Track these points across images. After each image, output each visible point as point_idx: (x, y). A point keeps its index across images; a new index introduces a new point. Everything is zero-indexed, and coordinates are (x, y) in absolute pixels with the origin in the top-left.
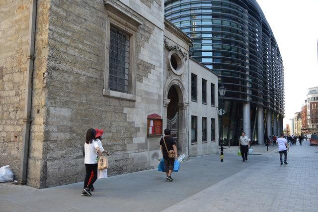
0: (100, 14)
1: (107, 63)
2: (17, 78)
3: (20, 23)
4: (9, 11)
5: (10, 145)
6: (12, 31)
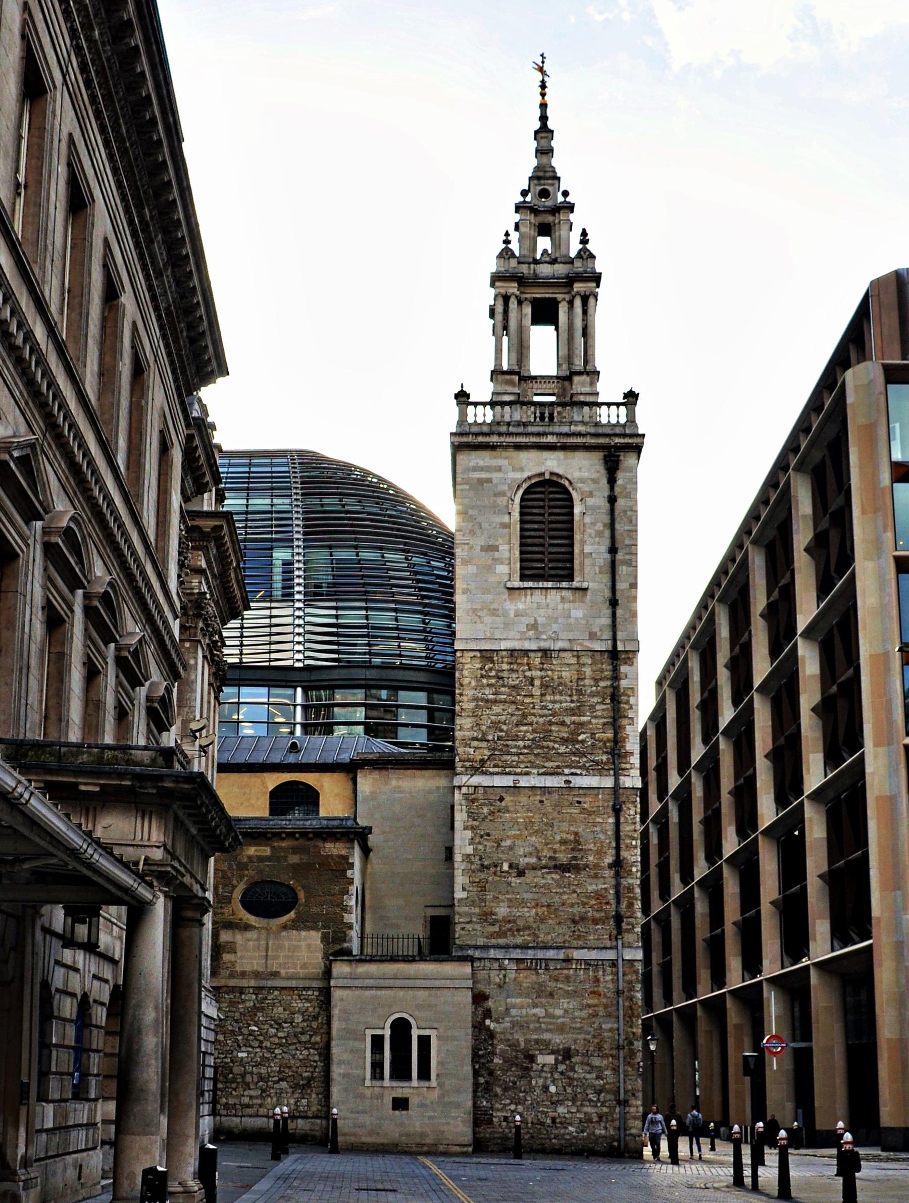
2: (596, 1062)
3: (596, 1009)
4: (575, 992)
5: (591, 1125)
6: (584, 1013)
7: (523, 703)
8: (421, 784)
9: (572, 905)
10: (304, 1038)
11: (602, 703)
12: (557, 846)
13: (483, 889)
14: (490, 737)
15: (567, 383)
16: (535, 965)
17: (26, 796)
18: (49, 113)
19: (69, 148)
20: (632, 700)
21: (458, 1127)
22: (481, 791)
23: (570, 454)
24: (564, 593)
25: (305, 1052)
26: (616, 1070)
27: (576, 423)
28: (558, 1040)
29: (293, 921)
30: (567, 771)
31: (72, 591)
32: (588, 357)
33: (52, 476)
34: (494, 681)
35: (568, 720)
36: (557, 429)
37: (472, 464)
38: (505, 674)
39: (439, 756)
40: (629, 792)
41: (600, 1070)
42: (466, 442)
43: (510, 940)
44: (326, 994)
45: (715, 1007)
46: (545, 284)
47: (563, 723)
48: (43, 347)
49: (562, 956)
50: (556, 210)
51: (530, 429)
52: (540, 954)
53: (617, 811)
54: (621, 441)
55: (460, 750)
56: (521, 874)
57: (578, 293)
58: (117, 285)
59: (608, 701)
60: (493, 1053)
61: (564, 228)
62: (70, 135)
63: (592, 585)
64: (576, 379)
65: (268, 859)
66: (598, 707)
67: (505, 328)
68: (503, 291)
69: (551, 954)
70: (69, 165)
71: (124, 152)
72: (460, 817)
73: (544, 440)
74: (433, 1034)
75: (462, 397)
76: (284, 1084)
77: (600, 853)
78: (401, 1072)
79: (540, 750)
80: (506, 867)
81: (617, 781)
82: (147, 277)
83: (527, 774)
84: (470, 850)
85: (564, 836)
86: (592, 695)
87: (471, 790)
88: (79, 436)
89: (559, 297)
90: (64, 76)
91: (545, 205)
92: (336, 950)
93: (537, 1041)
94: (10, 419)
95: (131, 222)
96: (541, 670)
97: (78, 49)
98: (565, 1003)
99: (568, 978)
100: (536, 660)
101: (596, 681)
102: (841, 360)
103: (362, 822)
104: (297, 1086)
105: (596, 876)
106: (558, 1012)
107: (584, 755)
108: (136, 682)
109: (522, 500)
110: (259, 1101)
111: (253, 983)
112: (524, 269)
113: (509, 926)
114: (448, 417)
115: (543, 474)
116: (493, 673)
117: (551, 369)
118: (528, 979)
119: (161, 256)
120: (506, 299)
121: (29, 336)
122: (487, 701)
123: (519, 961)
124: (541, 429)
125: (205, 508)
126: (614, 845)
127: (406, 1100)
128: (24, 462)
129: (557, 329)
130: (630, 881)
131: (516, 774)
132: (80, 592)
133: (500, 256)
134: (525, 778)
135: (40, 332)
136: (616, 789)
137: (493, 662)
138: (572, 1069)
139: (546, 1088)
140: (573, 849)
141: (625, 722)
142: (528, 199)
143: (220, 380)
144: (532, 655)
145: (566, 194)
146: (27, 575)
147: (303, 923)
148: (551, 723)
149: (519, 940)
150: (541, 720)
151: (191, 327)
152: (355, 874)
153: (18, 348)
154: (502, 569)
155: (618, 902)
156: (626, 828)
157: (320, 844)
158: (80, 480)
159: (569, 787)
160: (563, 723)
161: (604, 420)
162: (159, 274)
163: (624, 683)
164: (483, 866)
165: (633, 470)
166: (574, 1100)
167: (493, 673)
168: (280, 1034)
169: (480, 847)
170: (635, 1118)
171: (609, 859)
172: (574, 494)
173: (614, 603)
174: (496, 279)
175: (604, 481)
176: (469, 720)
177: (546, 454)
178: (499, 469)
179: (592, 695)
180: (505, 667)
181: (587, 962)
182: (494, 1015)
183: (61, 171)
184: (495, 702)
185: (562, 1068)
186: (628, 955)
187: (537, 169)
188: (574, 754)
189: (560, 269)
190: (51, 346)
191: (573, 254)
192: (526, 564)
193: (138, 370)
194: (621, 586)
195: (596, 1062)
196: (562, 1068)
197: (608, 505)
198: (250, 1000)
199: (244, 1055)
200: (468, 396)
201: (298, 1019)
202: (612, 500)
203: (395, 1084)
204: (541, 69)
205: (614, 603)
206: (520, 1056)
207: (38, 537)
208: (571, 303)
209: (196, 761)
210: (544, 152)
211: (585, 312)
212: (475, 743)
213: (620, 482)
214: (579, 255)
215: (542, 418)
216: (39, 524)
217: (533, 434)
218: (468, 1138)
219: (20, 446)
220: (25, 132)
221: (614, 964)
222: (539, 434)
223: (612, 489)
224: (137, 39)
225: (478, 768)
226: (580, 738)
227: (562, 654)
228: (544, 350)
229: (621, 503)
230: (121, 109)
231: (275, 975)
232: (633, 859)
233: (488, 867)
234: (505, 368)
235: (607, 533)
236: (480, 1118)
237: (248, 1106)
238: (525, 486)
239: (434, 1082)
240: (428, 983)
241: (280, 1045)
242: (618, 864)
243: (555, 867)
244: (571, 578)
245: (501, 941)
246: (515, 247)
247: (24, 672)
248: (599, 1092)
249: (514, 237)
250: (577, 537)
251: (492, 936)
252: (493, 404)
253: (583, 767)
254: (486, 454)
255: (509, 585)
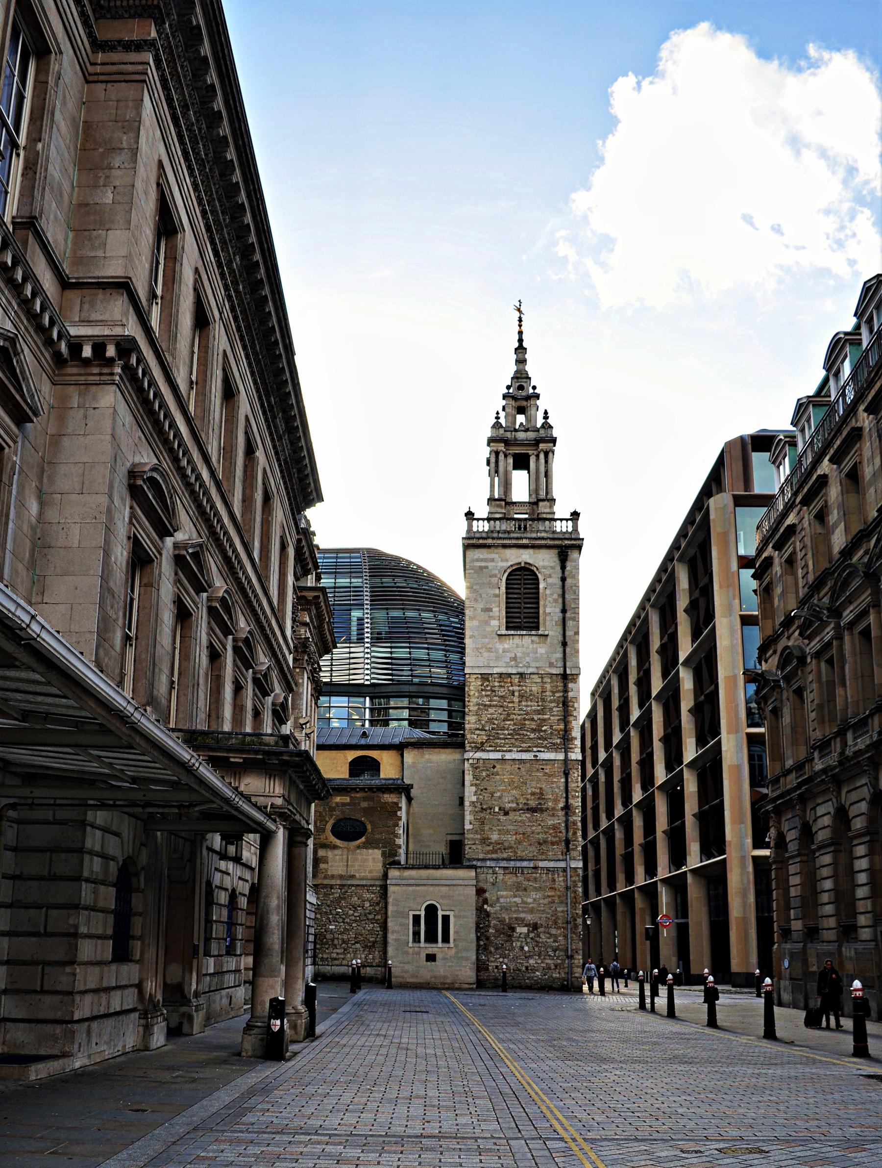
2: (553, 931)
6: (546, 901)
7: (507, 707)
8: (444, 758)
9: (538, 834)
10: (370, 917)
11: (557, 707)
12: (529, 796)
13: (483, 823)
14: (487, 728)
15: (535, 507)
16: (515, 871)
17: (197, 765)
18: (211, 337)
19: (224, 359)
20: (576, 705)
21: (468, 973)
22: (481, 762)
23: (537, 551)
24: (533, 638)
25: (371, 926)
26: (566, 937)
27: (541, 532)
28: (529, 917)
29: (364, 843)
30: (535, 749)
31: (226, 637)
32: (548, 490)
33: (213, 564)
34: (489, 693)
35: (536, 717)
36: (529, 535)
37: (476, 557)
38: (496, 689)
39: (455, 740)
40: (574, 763)
41: (556, 936)
42: (472, 543)
43: (500, 855)
44: (384, 888)
45: (628, 897)
46: (521, 444)
47: (533, 719)
48: (207, 484)
49: (532, 866)
50: (528, 398)
51: (512, 535)
52: (518, 864)
53: (566, 775)
54: (569, 542)
55: (468, 736)
56: (506, 814)
57: (542, 450)
58: (254, 445)
59: (561, 705)
60: (489, 926)
61: (534, 409)
62: (225, 351)
63: (551, 633)
64: (541, 504)
65: (348, 804)
66: (554, 709)
67: (497, 472)
68: (495, 449)
69: (525, 864)
70: (224, 370)
71: (258, 362)
72: (468, 778)
73: (520, 542)
74: (451, 914)
75: (469, 515)
76: (358, 946)
77: (556, 801)
78: (431, 938)
79: (518, 737)
80: (497, 809)
81: (566, 755)
82: (272, 440)
83: (510, 751)
84: (474, 799)
85: (533, 790)
86: (551, 702)
87: (475, 761)
88: (230, 539)
89: (530, 452)
90: (220, 314)
91: (521, 395)
92: (391, 861)
93: (516, 919)
94: (187, 529)
95: (262, 406)
96: (519, 686)
97: (229, 298)
98: (534, 894)
99: (535, 879)
100: (516, 680)
101: (554, 693)
102: (706, 492)
103: (407, 781)
104: (366, 946)
105: (553, 815)
106: (530, 900)
107: (546, 739)
108: (265, 694)
109: (507, 579)
110: (340, 956)
111: (338, 882)
112: (508, 435)
113: (499, 846)
114: (461, 528)
115: (520, 563)
116: (489, 688)
117: (525, 498)
118: (511, 879)
119: (281, 427)
120: (497, 453)
121: (199, 477)
122: (485, 705)
123: (505, 868)
124: (519, 535)
125: (309, 585)
126: (564, 795)
127: (435, 955)
128: (196, 556)
129: (529, 473)
130: (575, 818)
131: (503, 751)
132: (230, 637)
133: (493, 427)
134: (509, 754)
135: (205, 475)
136: (566, 760)
137: (489, 681)
138: (539, 936)
139: (522, 948)
140: (539, 798)
141: (571, 718)
142: (511, 391)
143: (318, 505)
144: (513, 676)
145: (534, 388)
146: (197, 627)
147: (370, 844)
148: (525, 719)
149: (505, 855)
150: (519, 717)
151: (300, 471)
152: (403, 814)
153: (192, 484)
154: (494, 623)
155: (567, 831)
156: (572, 785)
157: (381, 795)
158: (230, 567)
159: (536, 760)
160: (533, 719)
161: (558, 530)
162: (280, 438)
163: (571, 694)
164: (483, 809)
165: (576, 561)
166: (539, 956)
167: (489, 688)
168: (356, 914)
169: (481, 797)
170: (578, 967)
171: (561, 805)
172: (540, 576)
173: (564, 644)
174: (490, 441)
175: (558, 568)
176: (474, 717)
177: (522, 551)
178: (493, 560)
179: (551, 702)
180: (496, 684)
181: (548, 869)
182: (490, 902)
183: (219, 373)
184: (490, 706)
185: (532, 935)
186: (574, 864)
187: (516, 372)
188: (540, 739)
189: (531, 435)
190: (212, 483)
191: (539, 425)
192: (509, 620)
193: (267, 498)
194: (569, 633)
195: (553, 931)
196: (532, 935)
197: (560, 583)
198: (337, 892)
199: (333, 927)
200: (473, 514)
201: (367, 904)
202: (563, 579)
203: (427, 945)
204: (519, 310)
205: (564, 644)
206: (506, 928)
207: (204, 603)
208: (538, 456)
209: (303, 743)
210: (521, 361)
211: (546, 462)
212: (478, 732)
213: (568, 568)
214: (543, 426)
215: (520, 528)
216: (205, 595)
217: (514, 538)
218: (473, 979)
219: (193, 546)
220: (196, 349)
221: (564, 870)
222: (517, 538)
223: (563, 572)
224: (266, 291)
225: (480, 747)
226: (543, 729)
227: (532, 676)
228: (521, 486)
229: (569, 581)
230: (257, 334)
231: (353, 877)
232: (577, 804)
233: (486, 810)
234: (497, 497)
235: (560, 600)
236: (481, 967)
237: (335, 959)
238: (509, 571)
239: (452, 945)
240: (448, 882)
241: (356, 921)
242: (567, 808)
243: (528, 809)
244: (538, 628)
245: (494, 856)
246: (502, 421)
247: (196, 687)
248: (555, 951)
249: (502, 415)
250: (541, 603)
251: (488, 852)
252: (489, 519)
253: (545, 747)
254: (484, 551)
255: (499, 633)
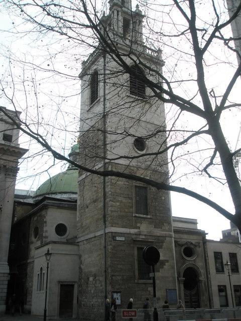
0: (132, 245)
1: (136, 267)
13: (81, 216)
28: (93, 270)
106: (93, 259)
138: (96, 283)
139: (91, 291)
